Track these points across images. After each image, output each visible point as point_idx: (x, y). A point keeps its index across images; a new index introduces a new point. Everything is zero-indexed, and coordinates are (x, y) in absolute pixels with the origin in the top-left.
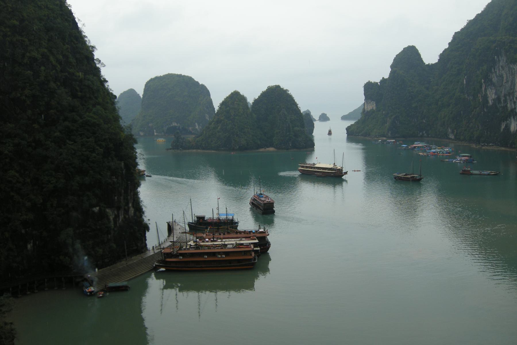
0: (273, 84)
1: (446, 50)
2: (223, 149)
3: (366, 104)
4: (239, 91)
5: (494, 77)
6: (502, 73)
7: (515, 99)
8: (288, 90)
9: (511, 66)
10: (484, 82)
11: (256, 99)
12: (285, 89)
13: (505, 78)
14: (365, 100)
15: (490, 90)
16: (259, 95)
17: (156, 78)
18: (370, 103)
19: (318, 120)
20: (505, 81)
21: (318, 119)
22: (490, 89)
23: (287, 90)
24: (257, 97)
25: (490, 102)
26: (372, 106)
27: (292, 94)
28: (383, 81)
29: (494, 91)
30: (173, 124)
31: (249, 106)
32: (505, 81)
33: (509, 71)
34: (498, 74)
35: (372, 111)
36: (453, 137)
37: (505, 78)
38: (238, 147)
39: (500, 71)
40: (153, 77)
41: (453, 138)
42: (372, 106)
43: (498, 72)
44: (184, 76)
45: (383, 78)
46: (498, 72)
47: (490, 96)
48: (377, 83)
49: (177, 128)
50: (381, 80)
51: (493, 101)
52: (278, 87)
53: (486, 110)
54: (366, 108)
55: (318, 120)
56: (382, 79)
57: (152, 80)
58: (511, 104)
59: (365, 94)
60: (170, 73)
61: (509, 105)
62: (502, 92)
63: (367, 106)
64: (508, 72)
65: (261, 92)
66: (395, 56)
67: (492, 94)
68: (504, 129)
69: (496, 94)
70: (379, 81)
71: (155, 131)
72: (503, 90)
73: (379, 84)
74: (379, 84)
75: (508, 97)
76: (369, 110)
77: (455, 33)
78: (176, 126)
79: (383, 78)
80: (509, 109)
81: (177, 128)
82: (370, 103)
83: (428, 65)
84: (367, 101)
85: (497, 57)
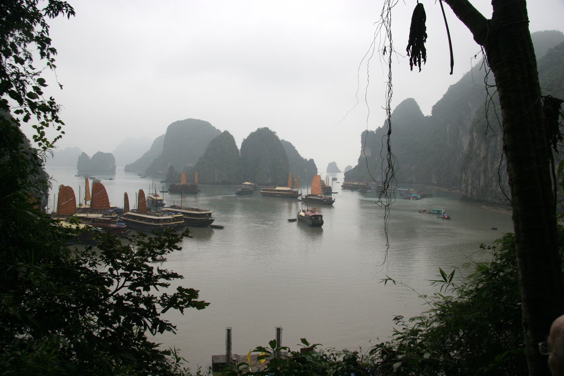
0: (262, 126)
4: (229, 131)
8: (275, 132)
11: (245, 139)
12: (273, 131)
14: (361, 147)
16: (248, 135)
17: (178, 122)
23: (274, 132)
24: (246, 138)
27: (278, 136)
31: (239, 145)
40: (175, 121)
44: (203, 121)
45: (379, 127)
48: (373, 132)
50: (377, 129)
52: (267, 129)
53: (461, 156)
56: (378, 128)
57: (173, 124)
60: (191, 118)
65: (250, 133)
67: (467, 140)
70: (375, 130)
73: (375, 132)
74: (375, 132)
79: (379, 127)
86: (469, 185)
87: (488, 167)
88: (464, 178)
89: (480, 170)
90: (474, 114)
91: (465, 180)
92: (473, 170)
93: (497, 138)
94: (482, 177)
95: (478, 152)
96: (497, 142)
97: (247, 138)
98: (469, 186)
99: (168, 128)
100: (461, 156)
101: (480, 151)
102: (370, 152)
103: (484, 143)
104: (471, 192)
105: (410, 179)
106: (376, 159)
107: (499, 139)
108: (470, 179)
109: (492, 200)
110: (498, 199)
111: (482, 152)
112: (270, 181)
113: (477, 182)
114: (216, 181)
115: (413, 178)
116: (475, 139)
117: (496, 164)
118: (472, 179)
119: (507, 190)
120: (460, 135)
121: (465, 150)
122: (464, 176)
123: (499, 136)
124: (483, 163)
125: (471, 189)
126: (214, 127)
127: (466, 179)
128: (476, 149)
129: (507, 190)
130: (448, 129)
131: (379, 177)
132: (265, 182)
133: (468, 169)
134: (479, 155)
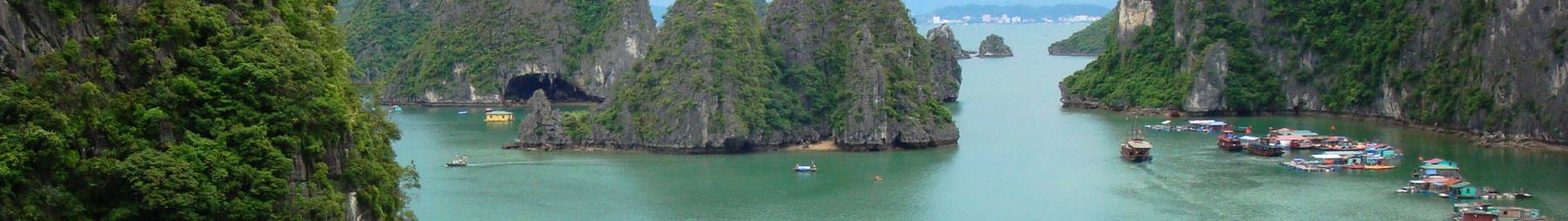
2: (676, 146)
30: (529, 70)
35: (1142, 33)
36: (1397, 113)
41: (1396, 117)
49: (541, 80)
53: (1503, 29)
54: (1122, 20)
63: (1127, 14)
71: (472, 89)
78: (538, 74)
81: (541, 80)
100: (1503, 29)
105: (1295, 101)
106: (1179, 35)
112: (883, 135)
114: (705, 141)
115: (1305, 98)
121: (1520, 9)
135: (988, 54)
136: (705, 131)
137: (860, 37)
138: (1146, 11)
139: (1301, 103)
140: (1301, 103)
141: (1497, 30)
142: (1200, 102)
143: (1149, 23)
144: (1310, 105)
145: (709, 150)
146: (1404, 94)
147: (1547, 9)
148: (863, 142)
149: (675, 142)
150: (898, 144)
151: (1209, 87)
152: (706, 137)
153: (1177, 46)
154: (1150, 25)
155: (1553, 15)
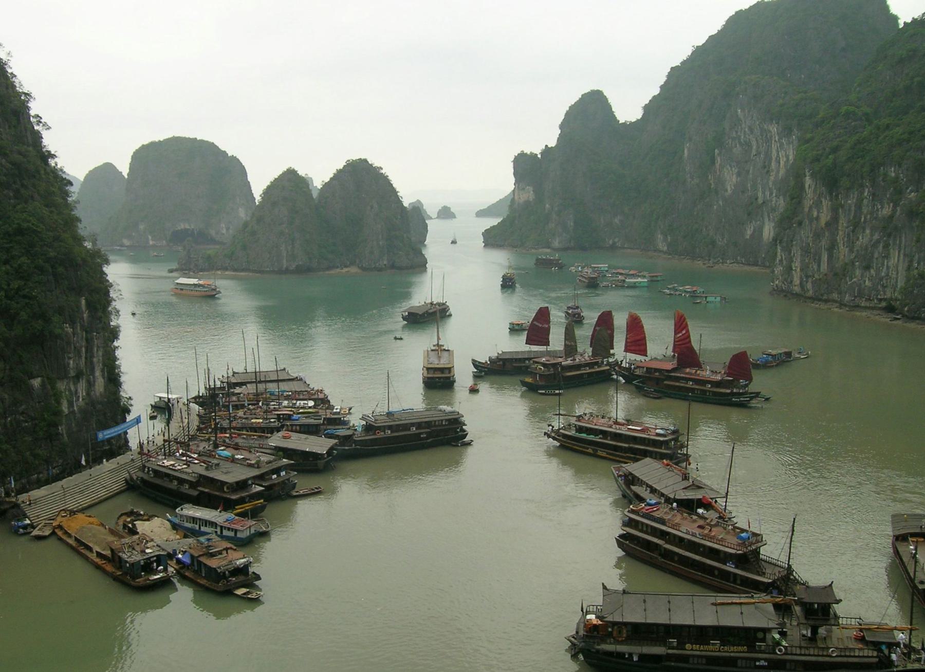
0: (355, 157)
1: (654, 97)
2: (268, 269)
3: (516, 191)
5: (736, 147)
6: (749, 139)
7: (771, 183)
9: (765, 127)
10: (719, 154)
13: (754, 147)
14: (515, 184)
15: (730, 169)
18: (523, 189)
19: (437, 218)
20: (754, 152)
21: (436, 216)
22: (728, 166)
25: (729, 189)
26: (529, 195)
28: (547, 151)
29: (735, 170)
31: (315, 195)
32: (754, 152)
33: (762, 136)
34: (742, 140)
35: (527, 203)
36: (665, 248)
37: (754, 147)
38: (294, 266)
39: (747, 136)
42: (529, 195)
43: (742, 137)
45: (546, 146)
46: (742, 137)
47: (728, 178)
51: (733, 188)
53: (721, 203)
54: (516, 198)
55: (437, 218)
58: (764, 193)
59: (515, 174)
61: (760, 194)
62: (749, 171)
64: (760, 137)
65: (335, 171)
66: (568, 109)
67: (733, 174)
68: (752, 236)
69: (739, 174)
72: (751, 168)
73: (539, 156)
74: (539, 156)
75: (759, 179)
76: (522, 201)
77: (672, 68)
80: (760, 201)
82: (523, 189)
83: (624, 124)
84: (519, 185)
85: (741, 112)
86: (796, 270)
87: (839, 241)
88: (779, 258)
89: (820, 245)
90: (747, 130)
91: (781, 261)
92: (804, 245)
93: (862, 193)
94: (825, 257)
95: (815, 214)
96: (863, 200)
97: (328, 180)
98: (794, 272)
99: (132, 157)
101: (818, 212)
102: (532, 192)
103: (828, 198)
104: (801, 283)
105: (611, 242)
107: (866, 194)
108: (799, 260)
109: (854, 300)
110: (864, 299)
111: (823, 214)
112: (385, 262)
113: (815, 267)
115: (616, 240)
116: (807, 190)
117: (861, 238)
118: (802, 261)
119: (883, 284)
120: (717, 165)
121: (729, 191)
122: (779, 254)
123: (867, 190)
124: (827, 234)
125: (801, 278)
126: (225, 152)
127: (783, 258)
128: (811, 208)
129: (883, 284)
130: (686, 151)
131: (557, 241)
132: (377, 264)
133: (794, 243)
134: (818, 218)
135: (442, 216)
136: (285, 261)
137: (372, 207)
138: (529, 192)
139: (614, 243)
140: (614, 243)
141: (717, 202)
142: (559, 243)
143: (531, 199)
144: (619, 244)
145: (287, 271)
146: (669, 238)
147: (743, 192)
148: (373, 266)
149: (268, 267)
150: (393, 267)
151: (564, 235)
152: (285, 264)
153: (547, 211)
154: (531, 200)
155: (746, 195)
